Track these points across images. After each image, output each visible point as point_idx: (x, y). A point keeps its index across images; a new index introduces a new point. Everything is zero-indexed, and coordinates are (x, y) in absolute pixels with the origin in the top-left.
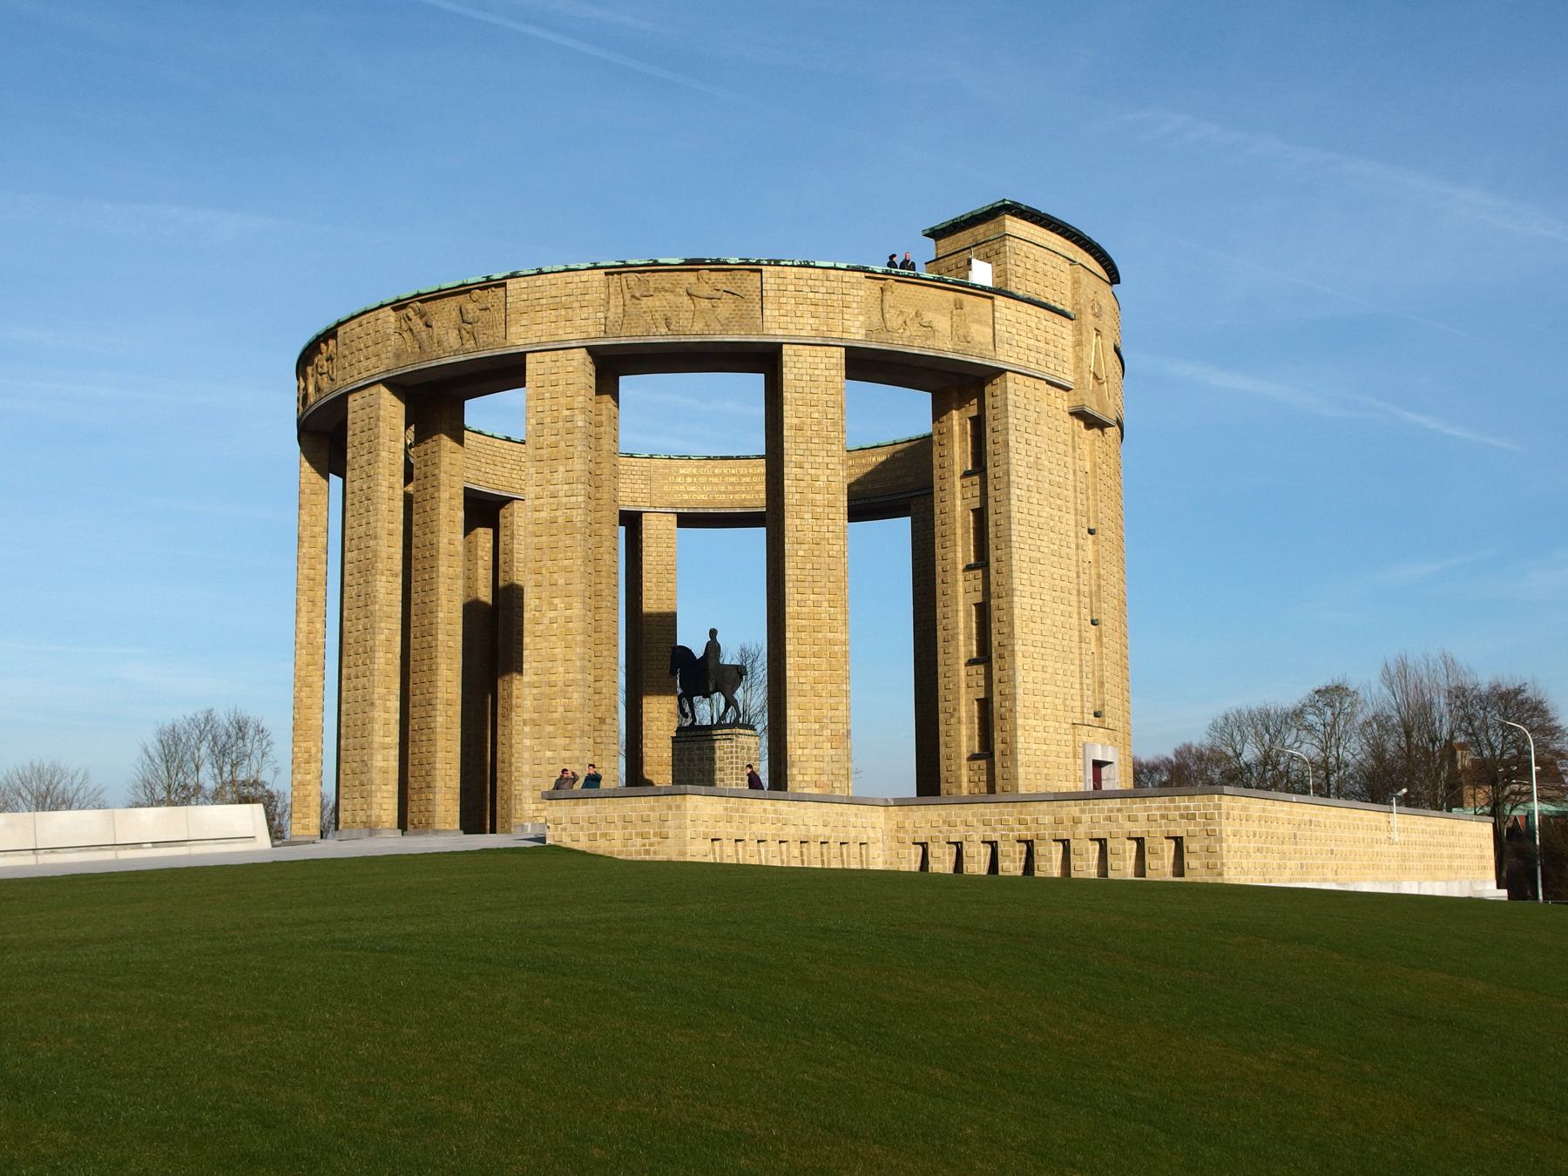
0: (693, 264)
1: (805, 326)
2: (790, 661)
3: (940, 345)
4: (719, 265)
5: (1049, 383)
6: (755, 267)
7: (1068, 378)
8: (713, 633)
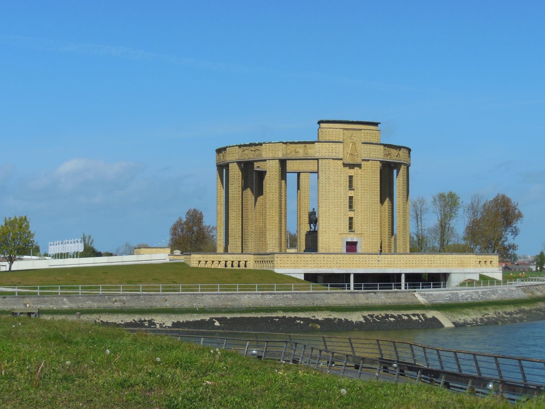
0: (251, 145)
1: (270, 156)
2: (230, 230)
3: (300, 156)
4: (255, 145)
5: (333, 159)
6: (261, 144)
7: (341, 156)
8: (314, 209)
